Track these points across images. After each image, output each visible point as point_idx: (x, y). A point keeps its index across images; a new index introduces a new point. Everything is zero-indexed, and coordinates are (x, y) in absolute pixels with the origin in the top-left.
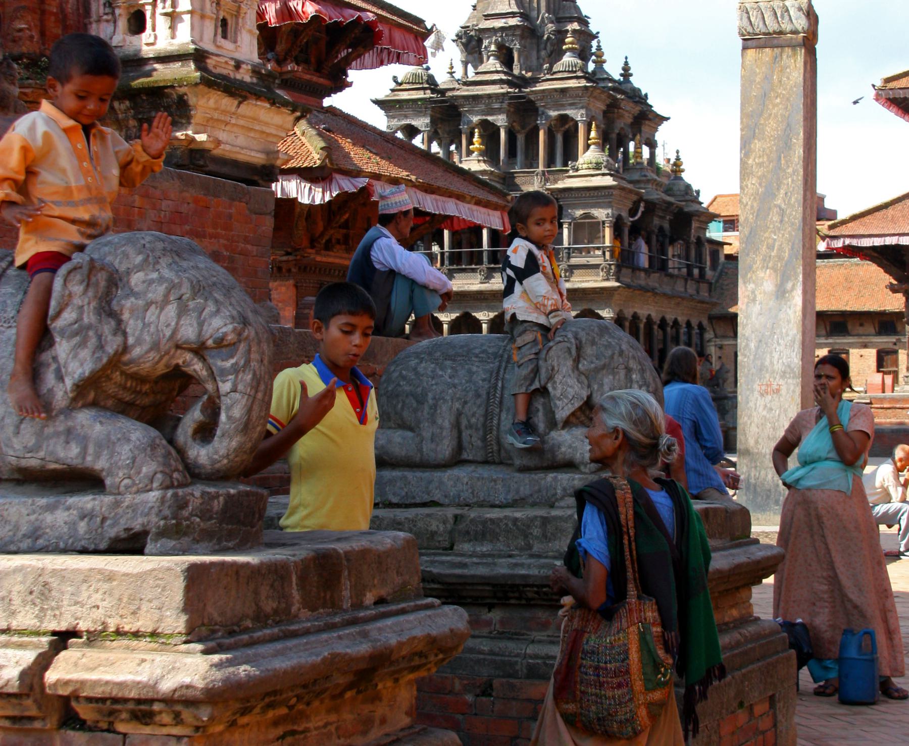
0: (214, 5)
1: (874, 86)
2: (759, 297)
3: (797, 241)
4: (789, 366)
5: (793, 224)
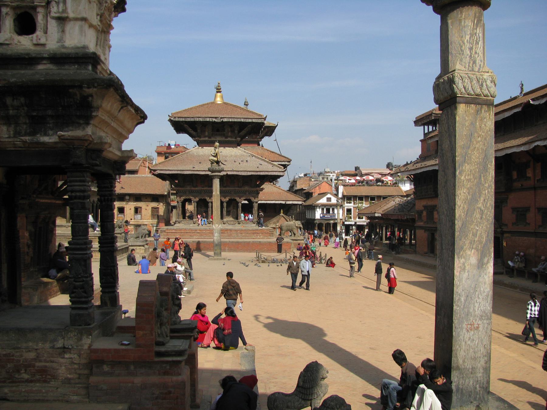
0: (99, 17)
1: (169, 116)
2: (467, 267)
3: (490, 231)
4: (484, 312)
5: (488, 220)
